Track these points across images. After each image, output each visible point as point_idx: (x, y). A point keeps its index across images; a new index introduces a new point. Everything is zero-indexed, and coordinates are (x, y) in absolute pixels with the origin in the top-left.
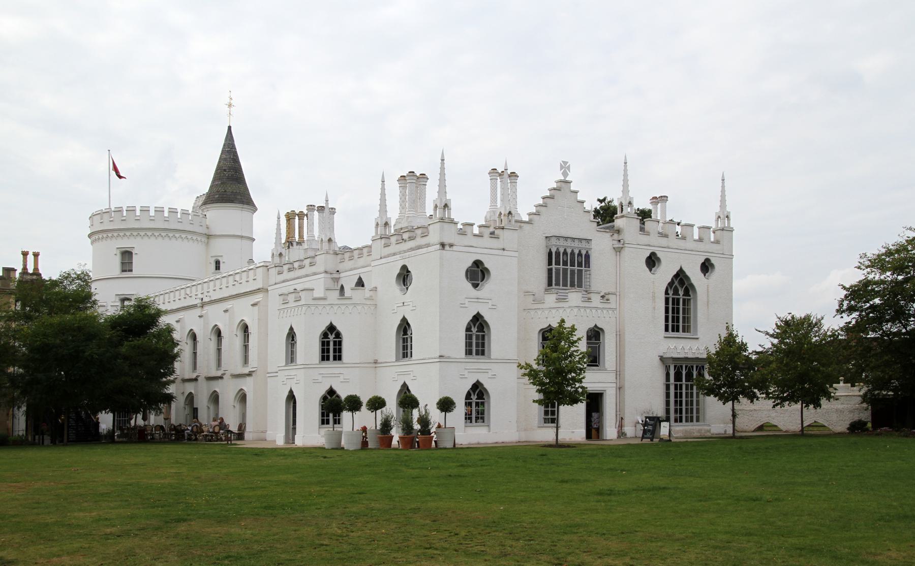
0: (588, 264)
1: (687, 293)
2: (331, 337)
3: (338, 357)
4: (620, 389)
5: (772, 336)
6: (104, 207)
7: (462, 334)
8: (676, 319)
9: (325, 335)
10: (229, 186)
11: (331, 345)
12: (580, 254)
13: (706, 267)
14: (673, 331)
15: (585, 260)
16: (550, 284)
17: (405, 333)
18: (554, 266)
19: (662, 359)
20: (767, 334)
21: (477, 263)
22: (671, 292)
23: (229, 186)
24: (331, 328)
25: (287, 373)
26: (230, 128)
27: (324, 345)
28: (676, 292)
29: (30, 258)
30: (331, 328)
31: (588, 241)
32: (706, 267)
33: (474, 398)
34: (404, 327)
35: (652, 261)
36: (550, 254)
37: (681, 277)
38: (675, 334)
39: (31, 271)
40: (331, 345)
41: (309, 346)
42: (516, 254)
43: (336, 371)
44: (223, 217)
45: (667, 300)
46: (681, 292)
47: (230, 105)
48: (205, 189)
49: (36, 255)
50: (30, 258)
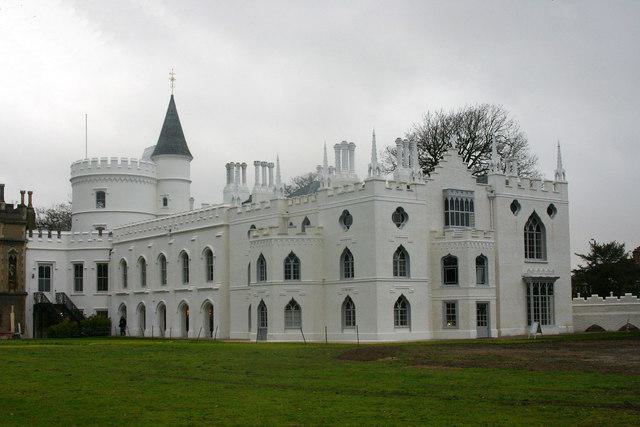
0: (472, 209)
1: (538, 230)
2: (292, 262)
3: (297, 276)
4: (497, 300)
5: (588, 259)
6: (82, 158)
7: (391, 261)
8: (531, 249)
9: (287, 260)
10: (172, 141)
11: (292, 267)
12: (467, 202)
13: (551, 210)
15: (470, 205)
16: (447, 223)
17: (347, 259)
18: (450, 211)
19: (525, 279)
20: (583, 257)
21: (400, 210)
22: (528, 229)
23: (172, 141)
24: (292, 256)
25: (258, 289)
26: (172, 96)
27: (287, 267)
28: (531, 229)
29: (26, 196)
30: (292, 256)
31: (472, 192)
32: (551, 210)
33: (399, 307)
34: (347, 256)
35: (515, 206)
36: (446, 202)
37: (534, 219)
38: (532, 260)
39: (26, 203)
40: (292, 267)
41: (276, 270)
43: (296, 287)
44: (171, 165)
45: (525, 234)
46: (534, 229)
47: (172, 80)
48: (154, 141)
49: (30, 194)
50: (26, 196)
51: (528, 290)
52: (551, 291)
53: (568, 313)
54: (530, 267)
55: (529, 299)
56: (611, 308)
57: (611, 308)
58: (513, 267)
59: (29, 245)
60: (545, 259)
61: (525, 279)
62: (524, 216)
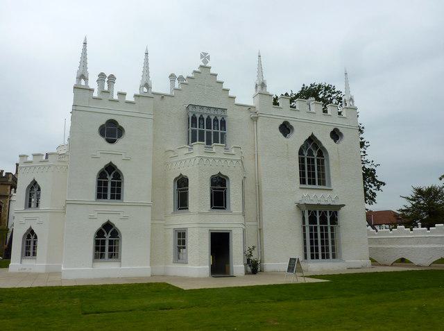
5: (412, 200)
8: (312, 175)
12: (216, 120)
13: (336, 135)
14: (309, 183)
19: (299, 206)
20: (408, 198)
22: (306, 154)
28: (310, 153)
31: (224, 110)
35: (286, 129)
37: (312, 141)
42: (152, 117)
51: (304, 218)
52: (334, 220)
53: (356, 251)
54: (305, 193)
55: (304, 228)
56: (419, 240)
57: (419, 240)
58: (285, 194)
59: (12, 199)
60: (330, 185)
61: (299, 206)
62: (298, 139)
